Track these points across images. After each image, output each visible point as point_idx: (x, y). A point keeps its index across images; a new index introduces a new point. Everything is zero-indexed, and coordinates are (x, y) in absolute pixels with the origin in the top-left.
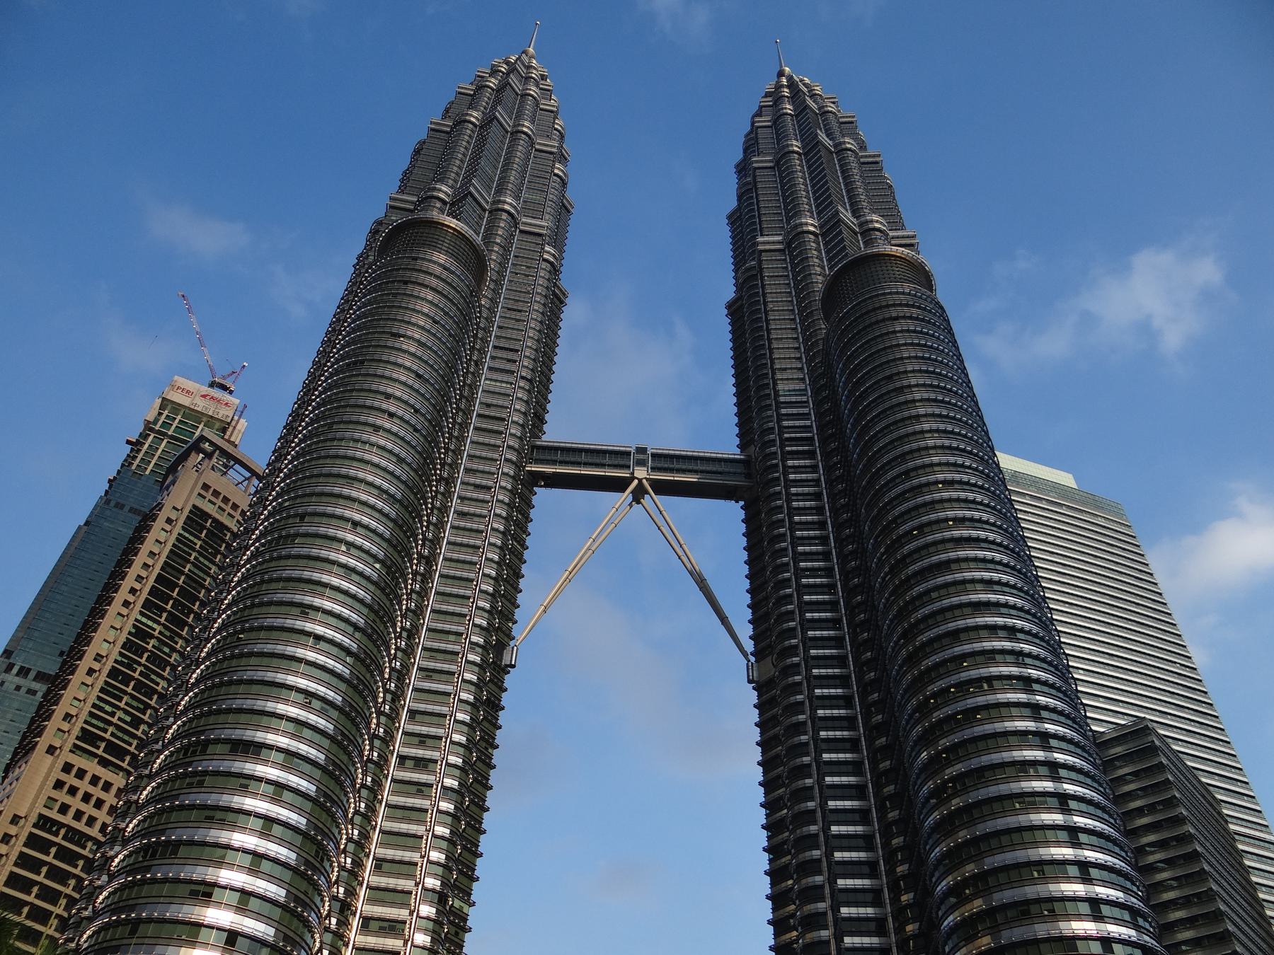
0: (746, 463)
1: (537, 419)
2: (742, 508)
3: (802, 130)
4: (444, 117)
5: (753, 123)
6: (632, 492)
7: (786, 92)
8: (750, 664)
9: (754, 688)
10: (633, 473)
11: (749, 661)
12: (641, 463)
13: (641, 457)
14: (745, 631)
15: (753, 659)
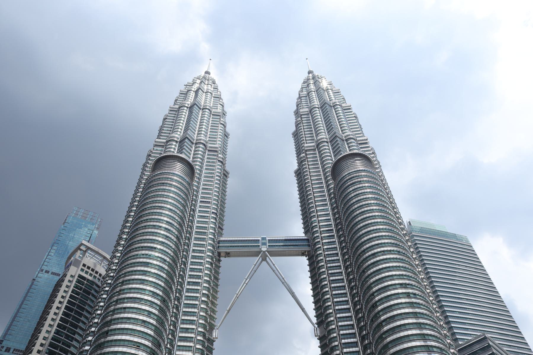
0: (307, 240)
1: (220, 228)
2: (307, 259)
3: (318, 95)
4: (175, 104)
5: (299, 95)
6: (261, 256)
7: (312, 82)
8: (315, 328)
9: (318, 339)
10: (261, 249)
11: (315, 327)
12: (264, 244)
13: (264, 241)
14: (312, 314)
15: (316, 326)
